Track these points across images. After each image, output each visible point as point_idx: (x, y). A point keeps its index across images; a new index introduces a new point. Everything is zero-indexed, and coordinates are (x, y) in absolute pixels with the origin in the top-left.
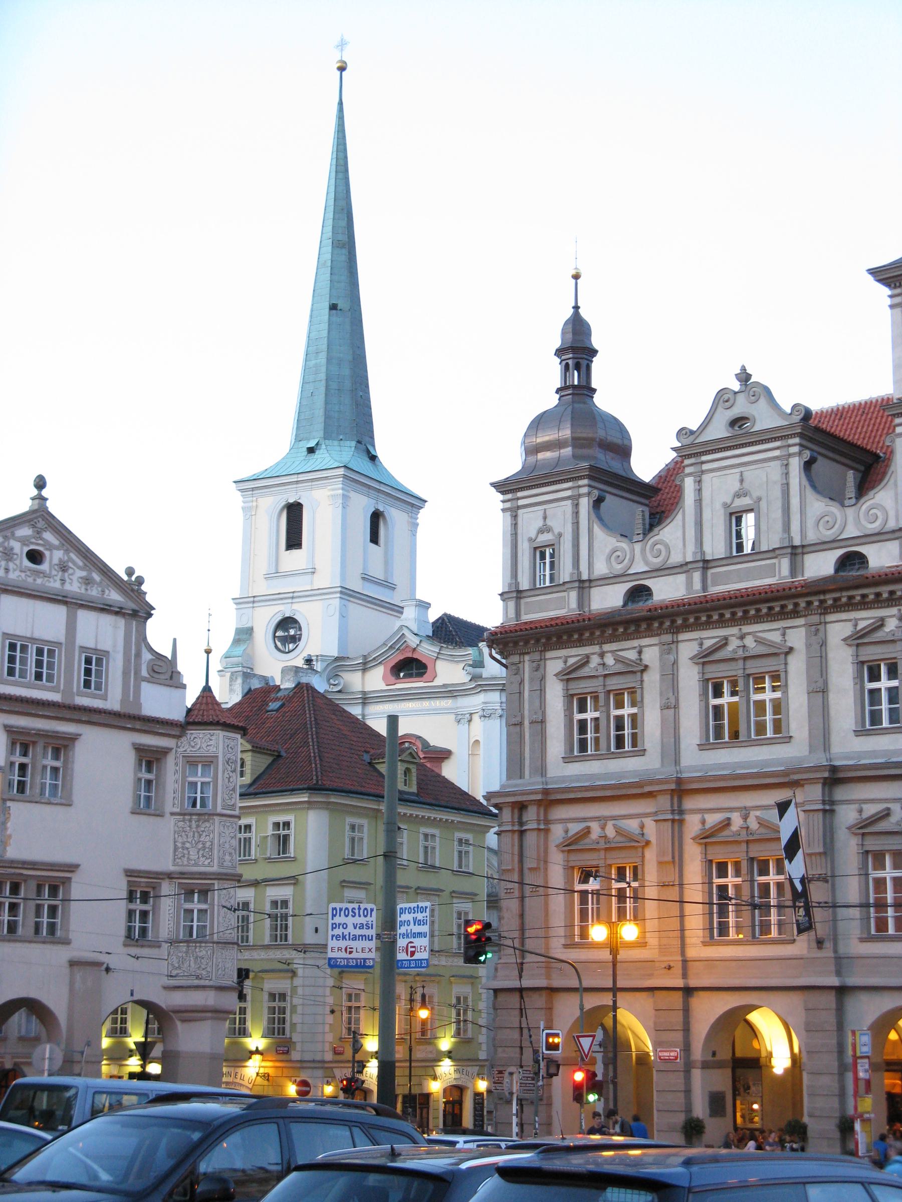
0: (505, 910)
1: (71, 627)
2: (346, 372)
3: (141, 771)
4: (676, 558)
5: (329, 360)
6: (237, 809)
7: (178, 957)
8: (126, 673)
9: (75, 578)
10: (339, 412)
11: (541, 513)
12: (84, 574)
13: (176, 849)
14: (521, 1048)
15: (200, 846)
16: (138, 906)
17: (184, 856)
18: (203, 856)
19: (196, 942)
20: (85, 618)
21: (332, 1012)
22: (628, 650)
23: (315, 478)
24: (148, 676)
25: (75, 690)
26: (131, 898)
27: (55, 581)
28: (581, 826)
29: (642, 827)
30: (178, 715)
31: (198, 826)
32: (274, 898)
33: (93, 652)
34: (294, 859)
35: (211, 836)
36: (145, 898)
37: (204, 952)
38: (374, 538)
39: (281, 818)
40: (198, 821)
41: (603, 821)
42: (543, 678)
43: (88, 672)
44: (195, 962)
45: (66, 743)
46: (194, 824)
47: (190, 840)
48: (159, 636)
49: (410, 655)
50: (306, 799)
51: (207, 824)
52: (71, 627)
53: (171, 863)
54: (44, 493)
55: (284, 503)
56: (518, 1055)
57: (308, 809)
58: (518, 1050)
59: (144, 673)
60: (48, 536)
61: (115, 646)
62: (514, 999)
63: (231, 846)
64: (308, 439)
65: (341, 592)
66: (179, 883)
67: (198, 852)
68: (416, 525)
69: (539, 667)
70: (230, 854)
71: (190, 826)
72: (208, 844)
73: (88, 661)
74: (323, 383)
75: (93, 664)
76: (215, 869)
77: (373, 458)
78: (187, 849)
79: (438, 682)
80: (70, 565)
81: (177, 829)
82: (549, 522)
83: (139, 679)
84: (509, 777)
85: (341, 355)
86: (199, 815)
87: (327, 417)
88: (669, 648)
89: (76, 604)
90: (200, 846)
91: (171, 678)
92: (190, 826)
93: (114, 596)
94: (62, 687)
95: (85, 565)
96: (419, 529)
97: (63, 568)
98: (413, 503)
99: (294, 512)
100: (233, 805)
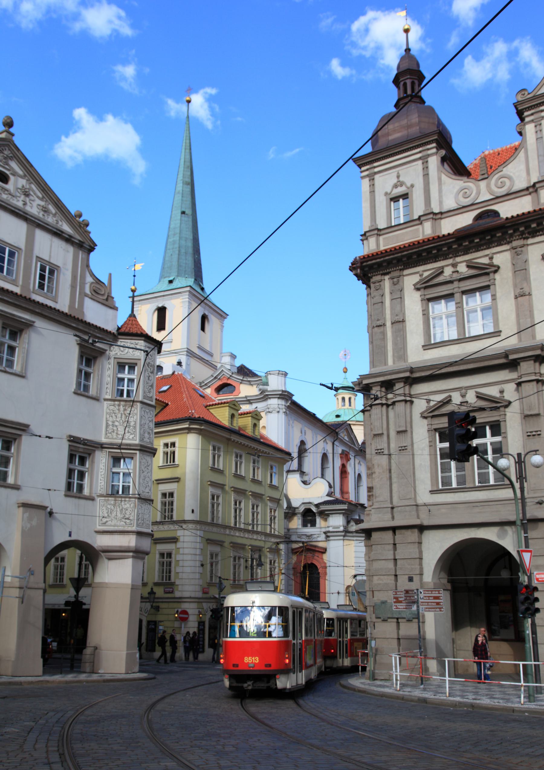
0: (376, 467)
1: (30, 240)
2: (190, 244)
3: (82, 364)
4: (521, 184)
5: (180, 238)
6: (154, 401)
7: (107, 509)
8: (73, 287)
9: (35, 204)
10: (186, 264)
11: (396, 174)
12: (42, 203)
14: (396, 576)
16: (77, 466)
17: (113, 432)
18: (128, 432)
19: (122, 497)
20: (41, 236)
21: (202, 565)
22: (481, 257)
23: (174, 293)
24: (90, 294)
25: (32, 289)
26: (71, 458)
27: (18, 201)
28: (446, 395)
29: (502, 392)
30: (111, 328)
31: (125, 410)
32: (164, 491)
33: (47, 263)
34: (178, 466)
35: (135, 417)
37: (128, 505)
38: (203, 329)
39: (169, 440)
40: (125, 406)
41: (463, 391)
42: (402, 290)
43: (42, 277)
44: (121, 512)
45: (22, 327)
46: (122, 408)
47: (117, 420)
48: (100, 264)
49: (225, 381)
50: (187, 426)
52: (30, 240)
54: (12, 130)
55: (155, 307)
56: (393, 582)
57: (188, 433)
58: (393, 578)
59: (87, 291)
60: (14, 165)
61: (65, 264)
63: (149, 427)
64: (169, 277)
65: (187, 351)
66: (109, 452)
68: (223, 326)
69: (396, 283)
70: (149, 433)
71: (119, 410)
73: (43, 269)
74: (178, 249)
75: (48, 273)
77: (203, 289)
78: (116, 426)
79: (241, 395)
80: (32, 193)
81: (108, 411)
82: (401, 179)
83: (83, 295)
84: (370, 368)
85: (187, 236)
86: (126, 401)
87: (179, 266)
88: (517, 252)
89: (34, 222)
91: (107, 300)
92: (119, 410)
93: (66, 228)
94: (21, 283)
95: (43, 197)
96: (224, 328)
97: (27, 195)
98: (222, 315)
99: (162, 312)
100: (151, 397)
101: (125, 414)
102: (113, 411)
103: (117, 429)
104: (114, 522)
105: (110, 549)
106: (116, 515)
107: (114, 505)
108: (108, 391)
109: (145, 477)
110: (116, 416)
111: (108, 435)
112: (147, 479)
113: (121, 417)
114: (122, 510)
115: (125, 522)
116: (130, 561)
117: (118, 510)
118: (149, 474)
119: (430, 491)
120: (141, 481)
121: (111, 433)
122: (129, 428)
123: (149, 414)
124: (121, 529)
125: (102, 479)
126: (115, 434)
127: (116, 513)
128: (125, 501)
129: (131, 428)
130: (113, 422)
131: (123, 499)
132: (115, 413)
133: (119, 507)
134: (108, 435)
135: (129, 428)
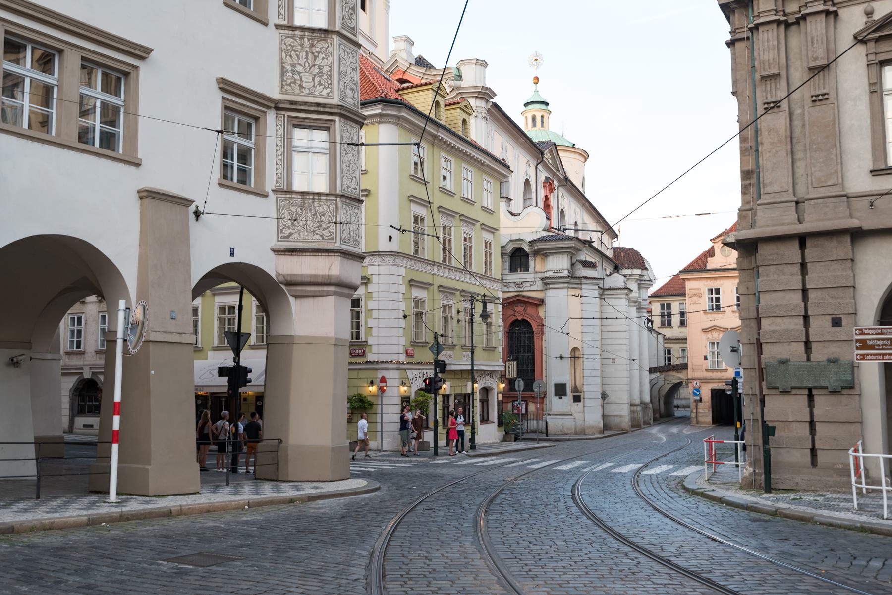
13: (283, 72)
15: (316, 70)
18: (320, 84)
31: (312, 46)
35: (330, 59)
36: (245, 132)
37: (325, 208)
47: (302, 62)
51: (323, 44)
53: (277, 90)
62: (792, 251)
66: (289, 117)
67: (313, 79)
71: (302, 45)
72: (326, 70)
76: (336, 101)
78: (299, 73)
81: (284, 47)
90: (316, 70)
101: (313, 53)
102: (293, 46)
103: (301, 78)
104: (304, 235)
105: (299, 279)
106: (306, 224)
107: (302, 207)
108: (282, 12)
109: (350, 161)
110: (298, 58)
111: (286, 87)
112: (354, 167)
113: (307, 58)
114: (315, 214)
115: (322, 236)
116: (331, 299)
117: (309, 215)
118: (355, 158)
119: (871, 171)
120: (344, 168)
121: (290, 85)
122: (321, 77)
123: (351, 56)
124: (315, 246)
125: (279, 162)
126: (297, 87)
127: (306, 221)
128: (320, 200)
129: (325, 77)
130: (293, 66)
131: (316, 197)
132: (295, 51)
133: (310, 211)
134: (286, 87)
135: (321, 77)
